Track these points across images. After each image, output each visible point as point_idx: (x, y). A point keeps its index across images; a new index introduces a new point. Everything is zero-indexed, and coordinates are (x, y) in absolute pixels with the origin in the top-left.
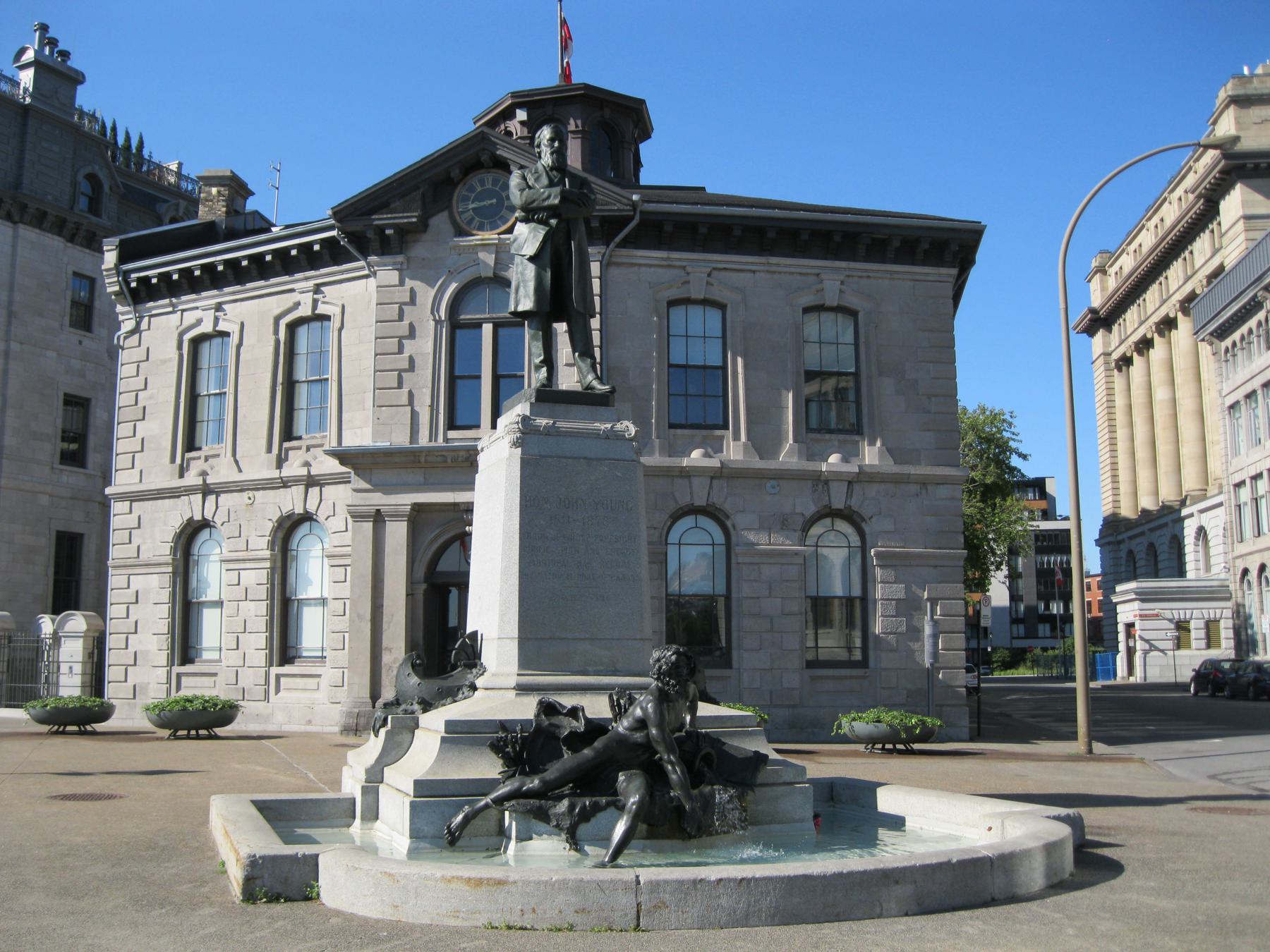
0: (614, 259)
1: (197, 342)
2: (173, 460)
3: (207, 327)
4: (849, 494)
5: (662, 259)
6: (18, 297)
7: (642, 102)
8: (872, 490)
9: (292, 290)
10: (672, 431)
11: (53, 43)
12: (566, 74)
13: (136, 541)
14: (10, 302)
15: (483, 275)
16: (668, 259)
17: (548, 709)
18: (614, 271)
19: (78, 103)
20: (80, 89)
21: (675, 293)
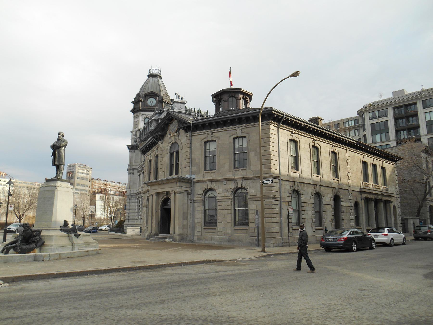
4: (242, 183)
7: (240, 89)
8: (248, 182)
18: (193, 137)
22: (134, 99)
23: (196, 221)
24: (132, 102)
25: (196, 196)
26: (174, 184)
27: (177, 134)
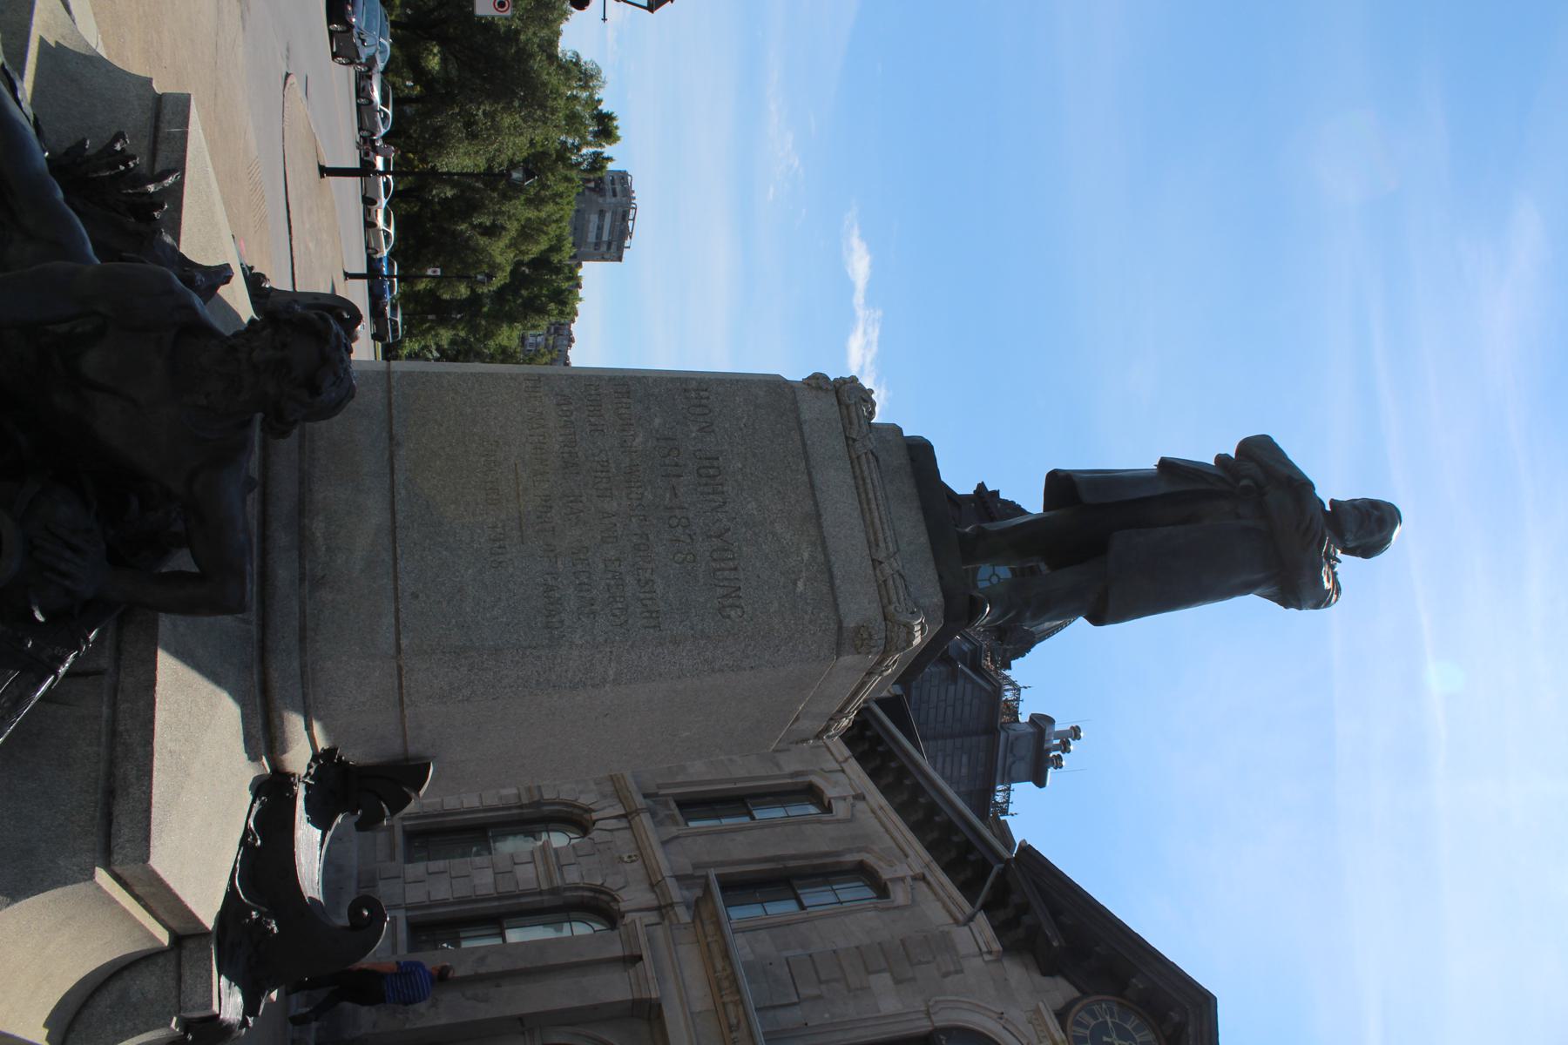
1: (811, 793)
3: (830, 792)
9: (906, 856)
11: (1065, 747)
19: (1013, 786)
20: (1030, 786)
22: (996, 493)
24: (981, 486)
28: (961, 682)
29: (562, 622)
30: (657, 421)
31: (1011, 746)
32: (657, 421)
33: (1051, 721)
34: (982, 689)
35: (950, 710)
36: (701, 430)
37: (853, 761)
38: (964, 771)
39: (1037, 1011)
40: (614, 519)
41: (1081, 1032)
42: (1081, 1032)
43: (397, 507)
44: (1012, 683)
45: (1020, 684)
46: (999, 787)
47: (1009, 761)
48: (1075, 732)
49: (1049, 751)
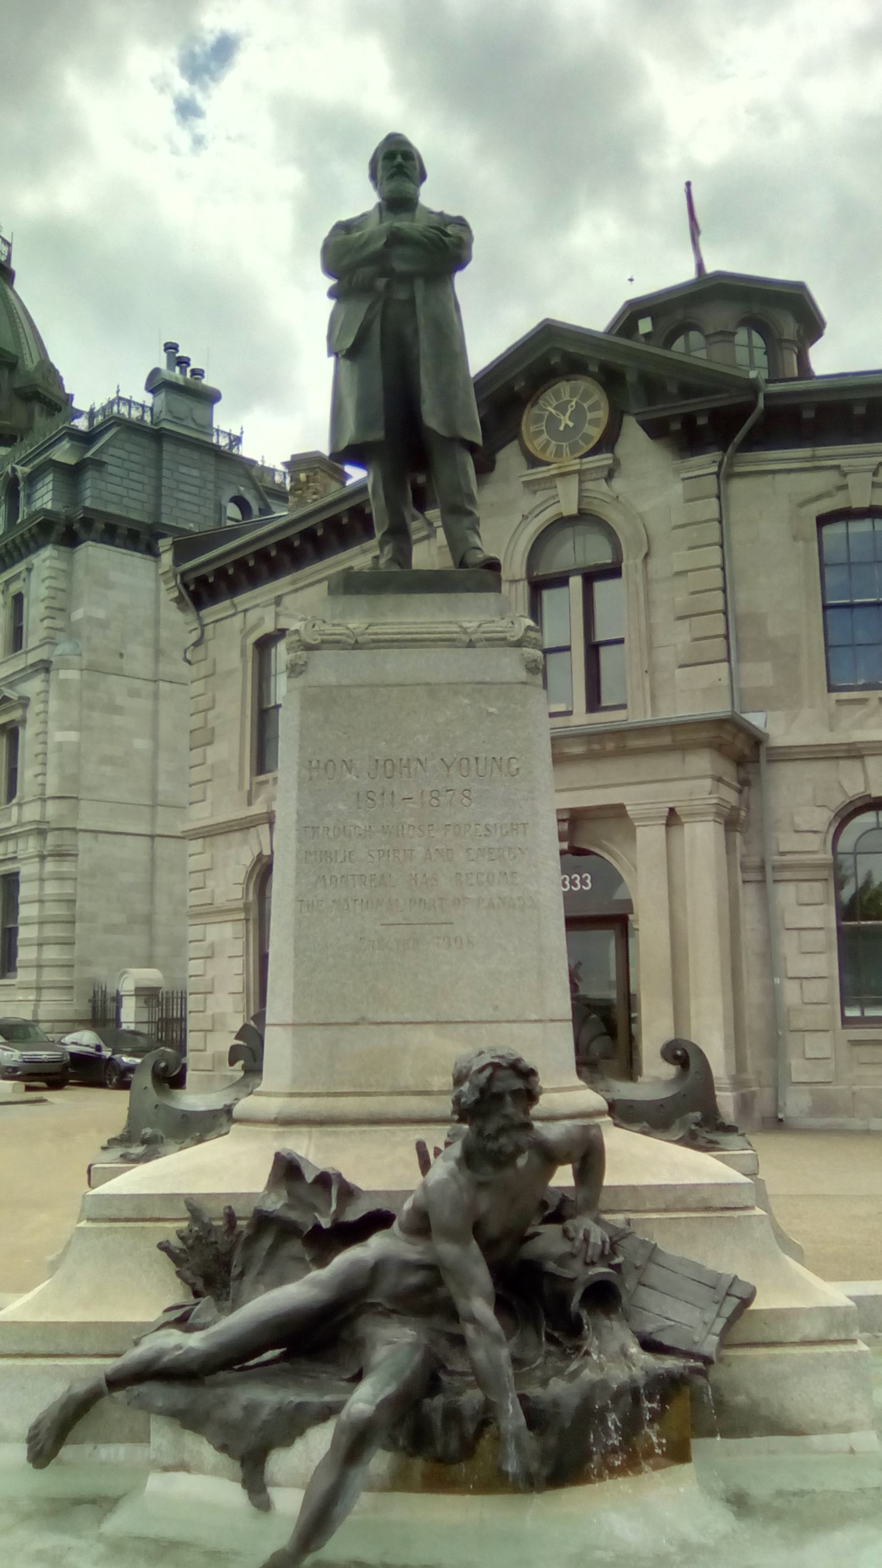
0: (737, 469)
2: (241, 786)
3: (268, 627)
5: (805, 459)
6: (164, 633)
7: (800, 287)
10: (835, 696)
11: (183, 362)
12: (700, 266)
13: (210, 884)
14: (157, 640)
15: (565, 514)
16: (813, 458)
17: (287, 1170)
18: (737, 487)
19: (215, 425)
20: (217, 407)
21: (826, 506)
23: (791, 994)
25: (787, 841)
26: (668, 764)
27: (604, 459)
28: (105, 458)
29: (519, 898)
30: (341, 807)
31: (178, 420)
32: (341, 807)
33: (155, 372)
34: (114, 437)
35: (133, 476)
36: (349, 770)
37: (237, 600)
38: (195, 473)
39: (527, 484)
40: (432, 851)
41: (552, 447)
42: (552, 447)
43: (420, 1019)
44: (111, 403)
45: (113, 396)
46: (214, 441)
47: (192, 425)
48: (171, 348)
49: (186, 380)
